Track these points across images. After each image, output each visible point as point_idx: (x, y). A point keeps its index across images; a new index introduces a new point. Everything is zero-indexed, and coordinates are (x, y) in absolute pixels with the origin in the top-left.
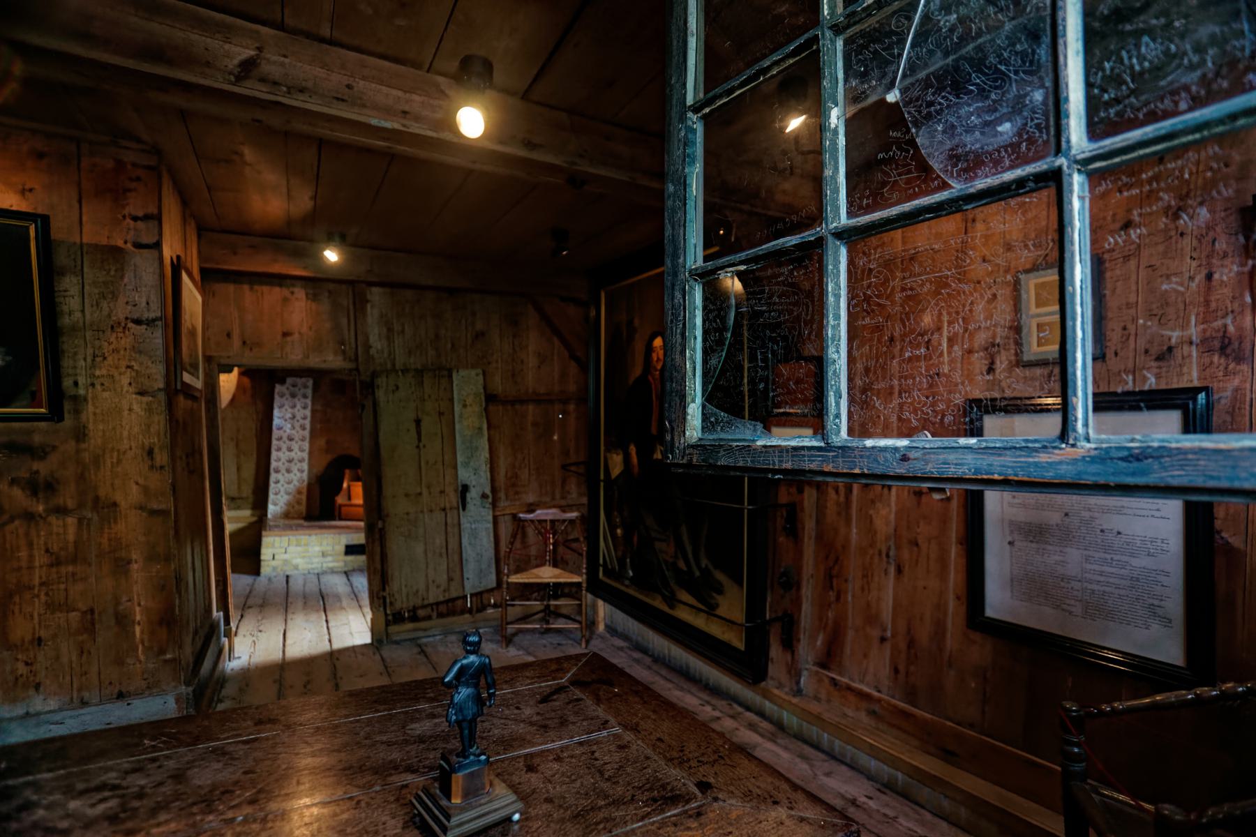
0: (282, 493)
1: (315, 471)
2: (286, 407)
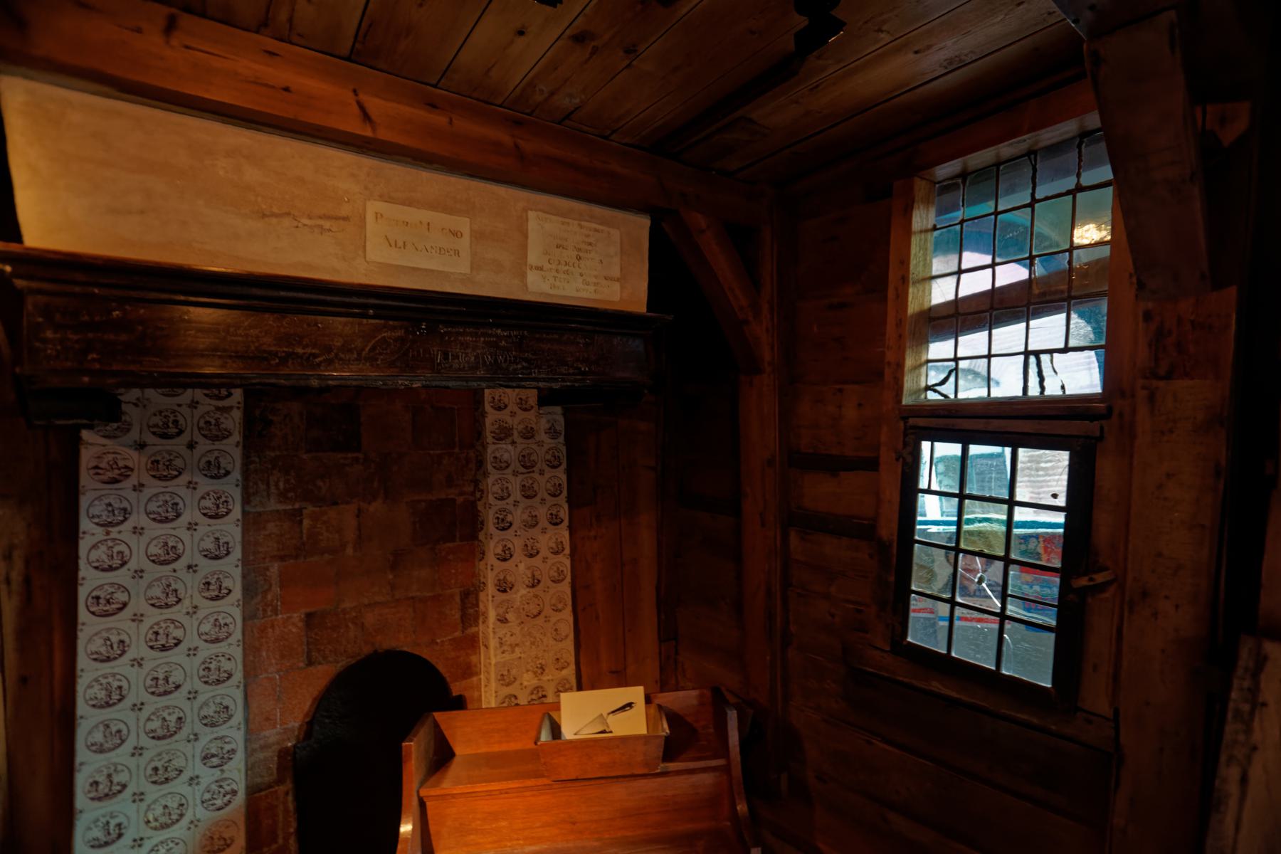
1: (272, 735)
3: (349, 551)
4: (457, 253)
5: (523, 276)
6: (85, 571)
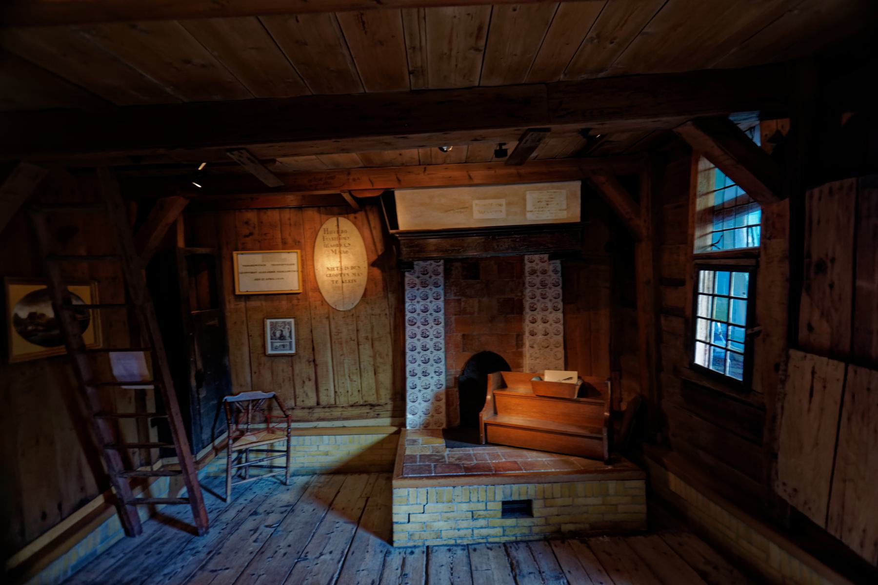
0: (420, 400)
1: (452, 371)
2: (418, 299)
3: (476, 314)
4: (501, 211)
5: (525, 215)
6: (407, 313)
